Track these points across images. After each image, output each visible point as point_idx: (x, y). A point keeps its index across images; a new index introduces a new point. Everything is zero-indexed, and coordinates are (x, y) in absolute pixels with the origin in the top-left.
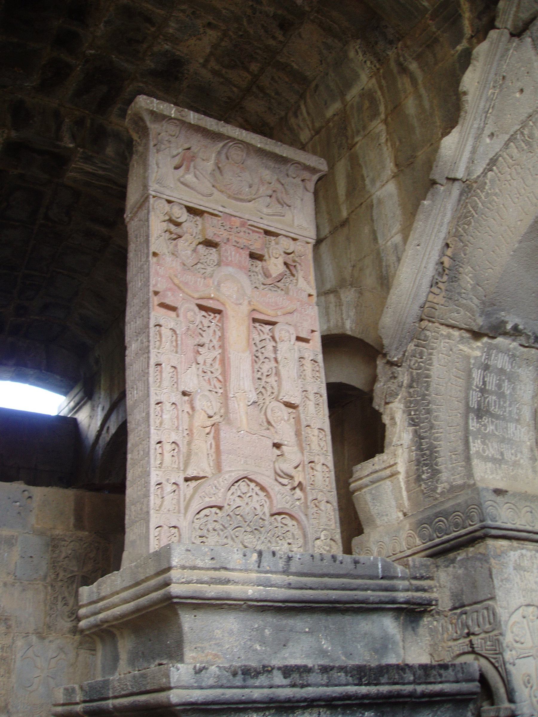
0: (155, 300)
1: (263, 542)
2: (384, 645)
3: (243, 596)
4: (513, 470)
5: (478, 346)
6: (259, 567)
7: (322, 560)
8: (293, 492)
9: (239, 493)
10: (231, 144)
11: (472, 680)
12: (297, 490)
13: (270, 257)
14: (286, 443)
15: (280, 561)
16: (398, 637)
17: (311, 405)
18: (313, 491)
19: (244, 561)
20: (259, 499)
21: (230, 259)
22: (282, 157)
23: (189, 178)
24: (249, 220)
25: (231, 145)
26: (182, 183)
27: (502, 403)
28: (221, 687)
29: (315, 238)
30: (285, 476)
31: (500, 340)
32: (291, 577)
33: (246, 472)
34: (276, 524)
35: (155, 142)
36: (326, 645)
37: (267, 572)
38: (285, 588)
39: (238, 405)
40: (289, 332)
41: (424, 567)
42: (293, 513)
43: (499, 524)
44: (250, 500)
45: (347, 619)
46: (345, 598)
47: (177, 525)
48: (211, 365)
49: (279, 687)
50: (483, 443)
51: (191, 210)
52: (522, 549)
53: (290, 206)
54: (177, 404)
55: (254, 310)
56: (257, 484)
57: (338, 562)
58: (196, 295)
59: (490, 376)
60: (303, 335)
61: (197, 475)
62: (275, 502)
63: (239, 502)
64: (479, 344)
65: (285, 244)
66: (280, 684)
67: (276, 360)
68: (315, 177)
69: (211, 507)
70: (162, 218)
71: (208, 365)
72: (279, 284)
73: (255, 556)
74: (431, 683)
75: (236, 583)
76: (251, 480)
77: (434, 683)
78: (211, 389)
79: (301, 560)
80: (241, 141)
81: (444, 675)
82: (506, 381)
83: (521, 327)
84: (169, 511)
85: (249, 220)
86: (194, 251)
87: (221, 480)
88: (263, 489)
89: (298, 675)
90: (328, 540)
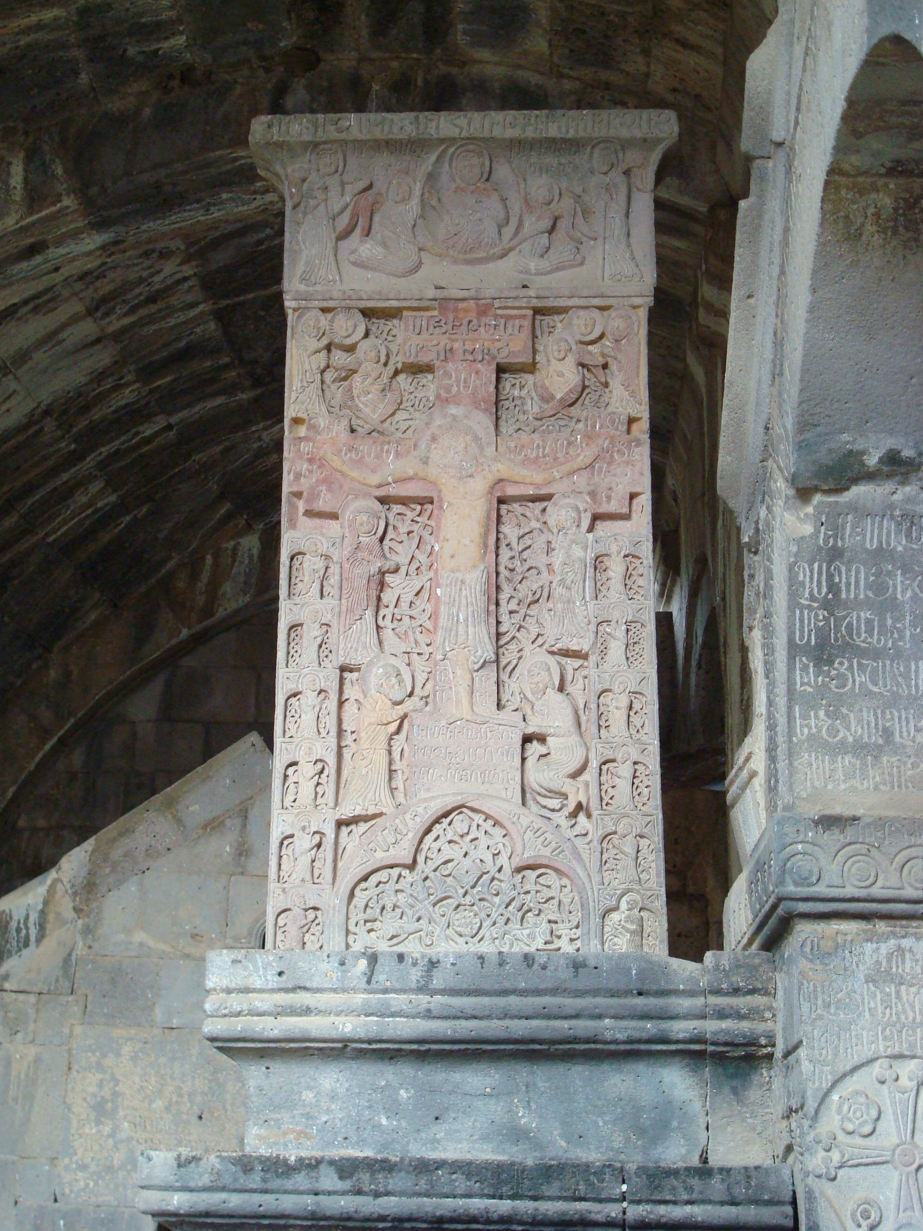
0: (301, 506)
1: (494, 924)
2: (660, 1121)
3: (334, 1034)
4: (914, 766)
5: (806, 515)
6: (369, 982)
7: (500, 965)
9: (450, 836)
10: (452, 150)
11: (780, 1203)
12: (582, 817)
13: (548, 361)
15: (413, 971)
16: (697, 1105)
17: (616, 649)
18: (607, 818)
20: (490, 843)
22: (564, 140)
23: (367, 249)
25: (453, 154)
26: (354, 264)
27: (889, 622)
28: (223, 1189)
31: (858, 491)
32: (438, 998)
35: (296, 200)
36: (525, 1118)
37: (385, 991)
38: (423, 1017)
41: (742, 970)
43: (820, 890)
45: (578, 1073)
46: (547, 1035)
49: (330, 1193)
50: (834, 715)
51: (367, 313)
52: (904, 937)
55: (501, 480)
56: (488, 817)
57: (536, 967)
58: (375, 480)
59: (848, 570)
60: (612, 507)
61: (364, 813)
62: (519, 846)
63: (449, 852)
64: (810, 510)
65: (581, 324)
66: (330, 1189)
68: (655, 157)
70: (315, 344)
71: (404, 605)
72: (575, 411)
73: (363, 964)
74: (665, 1202)
75: (320, 1012)
77: (675, 1203)
78: (409, 650)
79: (456, 968)
80: (468, 138)
81: (697, 1189)
82: (899, 572)
83: (907, 453)
84: (303, 880)
87: (408, 817)
88: (496, 823)
89: (368, 1175)
90: (636, 911)
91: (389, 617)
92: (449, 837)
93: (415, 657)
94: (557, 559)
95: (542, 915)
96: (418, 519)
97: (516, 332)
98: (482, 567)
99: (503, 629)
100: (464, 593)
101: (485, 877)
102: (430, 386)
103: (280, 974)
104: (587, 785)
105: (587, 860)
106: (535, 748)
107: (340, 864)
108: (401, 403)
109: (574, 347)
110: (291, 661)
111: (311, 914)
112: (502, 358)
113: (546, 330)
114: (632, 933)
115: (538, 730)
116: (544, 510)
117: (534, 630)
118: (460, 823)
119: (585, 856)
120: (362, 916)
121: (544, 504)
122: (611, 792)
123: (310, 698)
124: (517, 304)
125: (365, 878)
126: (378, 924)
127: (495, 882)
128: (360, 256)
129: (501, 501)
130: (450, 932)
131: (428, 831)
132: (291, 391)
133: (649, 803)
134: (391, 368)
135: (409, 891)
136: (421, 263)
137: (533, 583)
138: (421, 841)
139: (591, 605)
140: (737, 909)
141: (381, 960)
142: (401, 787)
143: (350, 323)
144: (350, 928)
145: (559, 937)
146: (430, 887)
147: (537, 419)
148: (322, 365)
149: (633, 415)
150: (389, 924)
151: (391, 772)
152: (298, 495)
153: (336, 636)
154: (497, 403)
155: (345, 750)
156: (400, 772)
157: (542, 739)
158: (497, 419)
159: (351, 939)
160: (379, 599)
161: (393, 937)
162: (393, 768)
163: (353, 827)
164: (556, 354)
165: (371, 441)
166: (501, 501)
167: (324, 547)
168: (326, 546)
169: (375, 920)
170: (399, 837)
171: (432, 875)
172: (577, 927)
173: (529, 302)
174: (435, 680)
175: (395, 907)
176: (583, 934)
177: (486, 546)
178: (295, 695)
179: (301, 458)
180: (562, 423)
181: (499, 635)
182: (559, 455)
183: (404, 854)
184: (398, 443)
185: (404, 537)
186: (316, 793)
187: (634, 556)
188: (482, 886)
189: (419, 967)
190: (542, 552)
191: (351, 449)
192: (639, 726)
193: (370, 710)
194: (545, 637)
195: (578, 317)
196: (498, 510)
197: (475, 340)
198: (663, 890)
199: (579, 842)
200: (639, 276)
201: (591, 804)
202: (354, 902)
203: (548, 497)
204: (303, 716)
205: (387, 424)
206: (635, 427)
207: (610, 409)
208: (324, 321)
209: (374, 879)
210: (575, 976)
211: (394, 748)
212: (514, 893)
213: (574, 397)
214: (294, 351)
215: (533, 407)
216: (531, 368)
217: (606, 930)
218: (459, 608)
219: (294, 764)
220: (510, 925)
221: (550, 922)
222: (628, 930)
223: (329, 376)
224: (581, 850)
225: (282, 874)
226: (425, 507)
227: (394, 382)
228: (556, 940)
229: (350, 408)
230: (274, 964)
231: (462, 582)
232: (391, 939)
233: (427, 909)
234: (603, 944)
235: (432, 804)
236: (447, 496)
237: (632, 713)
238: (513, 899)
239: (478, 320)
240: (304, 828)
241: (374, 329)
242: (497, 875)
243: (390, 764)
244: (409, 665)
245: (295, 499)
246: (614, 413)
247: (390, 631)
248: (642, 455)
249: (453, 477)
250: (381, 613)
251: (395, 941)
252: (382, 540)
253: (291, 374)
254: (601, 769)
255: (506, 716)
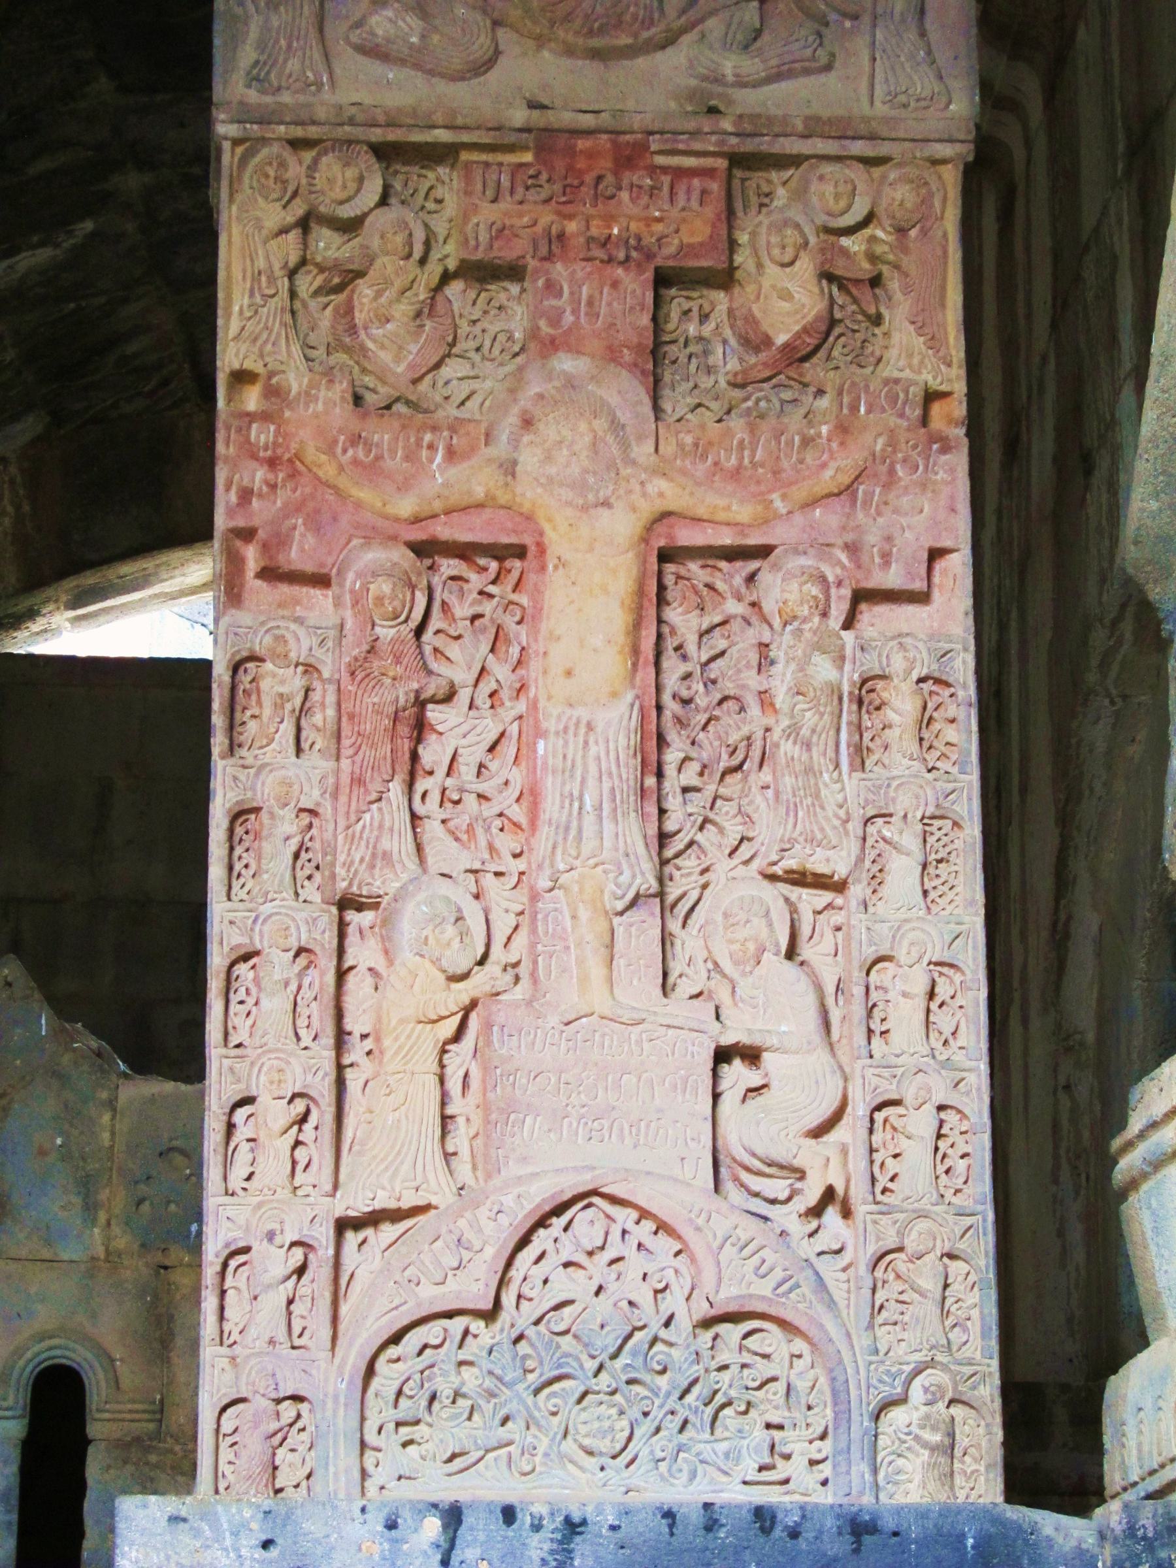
0: (252, 556)
8: (814, 1224)
12: (832, 1215)
13: (760, 266)
14: (773, 1041)
15: (535, 1540)
18: (884, 1220)
19: (386, 1546)
20: (650, 1268)
21: (569, 318)
24: (651, 133)
26: (361, 49)
29: (971, 137)
30: (767, 1170)
33: (588, 1176)
34: (723, 1357)
39: (574, 917)
40: (823, 579)
42: (788, 1316)
44: (614, 1276)
47: (302, 1393)
48: (481, 766)
53: (855, 17)
54: (317, 949)
55: (666, 515)
56: (644, 1215)
57: (778, 1532)
58: (406, 506)
60: (892, 578)
61: (393, 1205)
63: (564, 1285)
67: (765, 699)
69: (449, 1315)
70: (274, 215)
71: (467, 771)
73: (433, 1526)
76: (614, 1200)
78: (477, 865)
79: (619, 1535)
84: (272, 1342)
85: (651, 133)
86: (428, 309)
87: (483, 1213)
88: (662, 1227)
90: (941, 1405)
91: (434, 797)
92: (564, 1258)
93: (488, 880)
94: (780, 682)
95: (753, 1413)
96: (492, 589)
97: (694, 204)
98: (629, 696)
99: (670, 826)
100: (593, 750)
101: (638, 1335)
102: (514, 311)
103: (267, 1544)
104: (844, 1151)
105: (842, 1304)
106: (737, 1074)
107: (344, 1309)
108: (452, 345)
109: (813, 240)
110: (236, 885)
111: (288, 1411)
112: (667, 255)
113: (754, 200)
114: (933, 1449)
115: (746, 1040)
116: (751, 578)
117: (734, 831)
118: (587, 1225)
119: (839, 1294)
120: (391, 1415)
121: (753, 565)
122: (892, 1166)
123: (278, 964)
124: (697, 146)
125: (396, 1339)
126: (422, 1427)
127: (659, 1347)
128: (374, 34)
129: (665, 556)
130: (569, 1446)
131: (524, 1242)
132: (229, 316)
133: (967, 1190)
134: (434, 270)
135: (485, 1364)
136: (497, 53)
137: (732, 727)
138: (509, 1264)
139: (852, 783)
140: (1148, 1404)
141: (468, 1520)
142: (465, 1153)
143: (351, 173)
144: (367, 1438)
145: (787, 1457)
146: (525, 1357)
147: (734, 385)
148: (293, 260)
149: (935, 385)
150: (444, 1431)
151: (445, 1119)
152: (247, 534)
153: (328, 835)
154: (656, 352)
155: (349, 1074)
156: (461, 1120)
157: (752, 1055)
158: (657, 382)
159: (370, 1458)
160: (415, 757)
161: (454, 1456)
162: (449, 1111)
163: (369, 1232)
164: (776, 252)
165: (396, 424)
166: (665, 556)
167: (302, 644)
168: (305, 643)
169: (417, 1422)
170: (467, 1256)
171: (531, 1332)
172: (823, 1437)
173: (722, 143)
174: (534, 931)
175: (457, 1395)
176: (837, 1452)
177: (636, 651)
178: (246, 957)
179: (254, 457)
180: (787, 395)
181: (663, 838)
182: (785, 464)
183: (475, 1289)
184: (453, 429)
185: (463, 626)
186: (294, 1163)
187: (938, 681)
188: (634, 1354)
189: (545, 1534)
190: (748, 666)
191: (355, 439)
192: (947, 1032)
193: (402, 992)
194: (755, 845)
195: (821, 178)
196: (660, 574)
197: (609, 219)
198: (995, 1364)
199: (826, 1266)
200: (944, 100)
201: (852, 1191)
202: (375, 1383)
203: (764, 551)
204: (265, 1003)
205: (424, 386)
206: (936, 408)
207: (887, 371)
208: (296, 170)
209: (413, 1340)
210: (856, 1551)
211: (449, 1071)
212: (696, 1370)
213: (812, 341)
214: (235, 230)
215: (728, 360)
216: (726, 279)
217: (882, 1441)
218: (583, 781)
219: (248, 1101)
220: (690, 1432)
221: (768, 1426)
222: (925, 1445)
223: (306, 283)
224: (830, 1284)
225: (226, 1329)
226: (508, 564)
227: (439, 298)
228: (780, 1463)
229: (348, 350)
230: (254, 1526)
231: (590, 727)
232: (450, 1460)
233: (522, 1401)
234: (875, 1471)
235: (533, 1189)
236: (557, 542)
237: (934, 1006)
238: (695, 1381)
239: (616, 173)
240: (271, 1236)
241: (398, 185)
242: (663, 1334)
243: (443, 1104)
244: (477, 897)
245: (238, 543)
246: (897, 381)
247: (437, 824)
248: (952, 471)
249: (569, 504)
250: (421, 786)
251: (458, 1463)
252: (419, 631)
253: (229, 278)
254: (872, 1121)
255: (678, 1008)
